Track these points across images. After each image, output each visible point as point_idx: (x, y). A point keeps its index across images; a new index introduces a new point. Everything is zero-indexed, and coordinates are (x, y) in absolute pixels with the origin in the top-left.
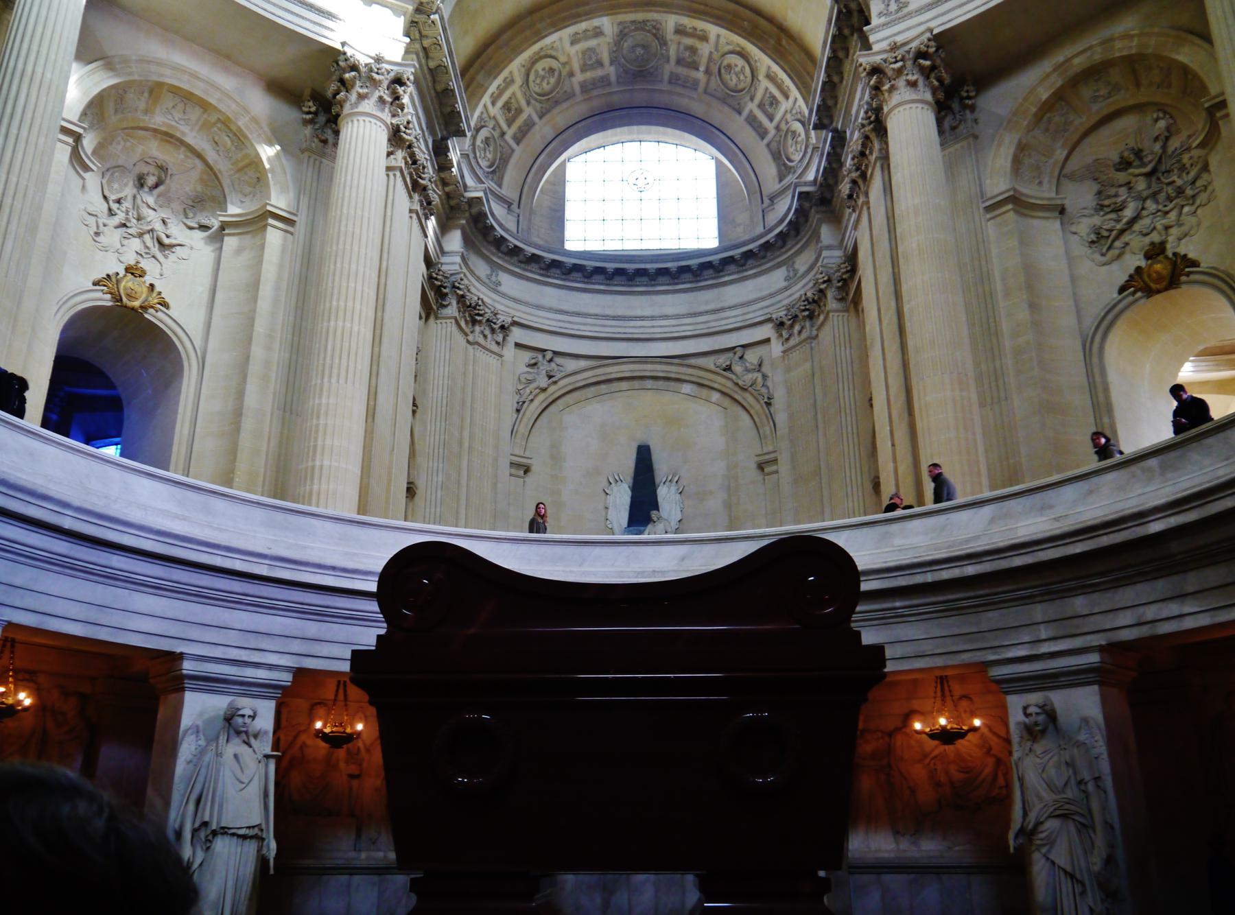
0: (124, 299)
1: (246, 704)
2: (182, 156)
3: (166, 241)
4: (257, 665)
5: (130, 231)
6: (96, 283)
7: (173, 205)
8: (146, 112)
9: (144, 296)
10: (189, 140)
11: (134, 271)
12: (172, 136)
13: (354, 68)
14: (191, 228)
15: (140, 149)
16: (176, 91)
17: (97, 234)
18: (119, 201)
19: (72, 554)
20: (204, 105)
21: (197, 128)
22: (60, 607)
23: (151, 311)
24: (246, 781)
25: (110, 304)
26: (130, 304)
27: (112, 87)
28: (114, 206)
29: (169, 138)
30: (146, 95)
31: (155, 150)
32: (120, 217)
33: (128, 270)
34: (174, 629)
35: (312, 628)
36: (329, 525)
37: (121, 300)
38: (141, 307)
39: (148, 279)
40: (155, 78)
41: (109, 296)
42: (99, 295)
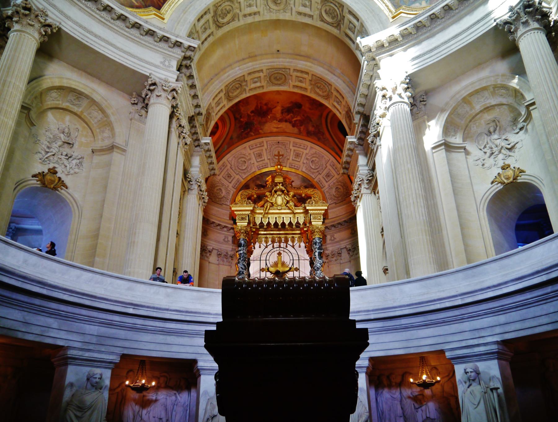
0: (506, 181)
1: (482, 366)
2: (498, 110)
3: (509, 147)
4: (478, 345)
5: (495, 154)
6: (492, 183)
7: (507, 130)
8: (471, 110)
9: (513, 174)
10: (493, 103)
11: (505, 167)
12: (488, 107)
13: (506, 23)
14: (518, 133)
15: (482, 122)
16: (471, 95)
17: (483, 165)
18: (485, 147)
19: (385, 325)
20: (484, 89)
21: (491, 97)
22: (391, 346)
23: (519, 178)
24: (476, 403)
25: (502, 187)
26: (509, 181)
27: (448, 115)
28: (485, 150)
29: (488, 109)
30: (465, 105)
31: (488, 117)
32: (489, 152)
33: (503, 168)
34: (440, 340)
35: (502, 318)
36: (493, 265)
37: (504, 183)
38: (514, 179)
39: (512, 167)
40: (460, 99)
41: (500, 184)
42: (496, 186)
